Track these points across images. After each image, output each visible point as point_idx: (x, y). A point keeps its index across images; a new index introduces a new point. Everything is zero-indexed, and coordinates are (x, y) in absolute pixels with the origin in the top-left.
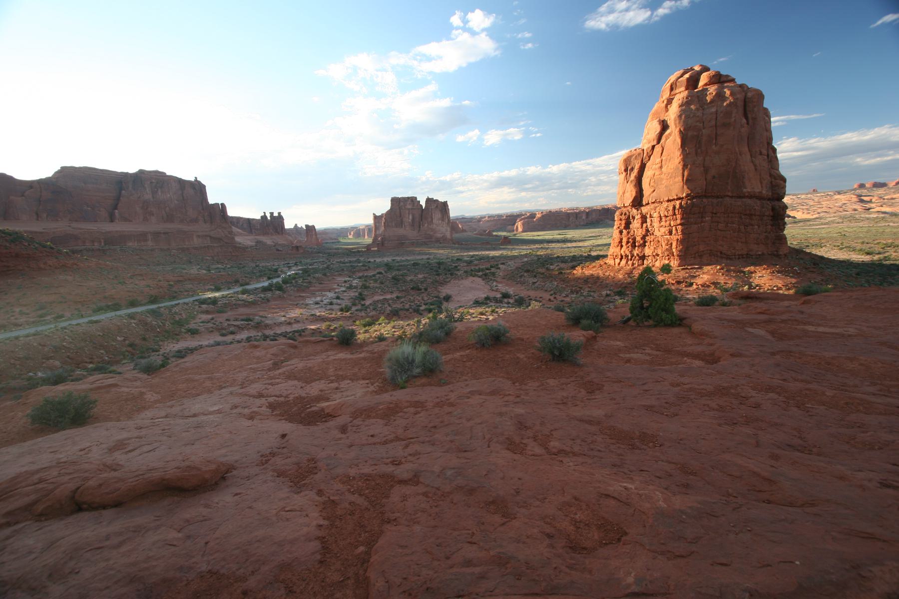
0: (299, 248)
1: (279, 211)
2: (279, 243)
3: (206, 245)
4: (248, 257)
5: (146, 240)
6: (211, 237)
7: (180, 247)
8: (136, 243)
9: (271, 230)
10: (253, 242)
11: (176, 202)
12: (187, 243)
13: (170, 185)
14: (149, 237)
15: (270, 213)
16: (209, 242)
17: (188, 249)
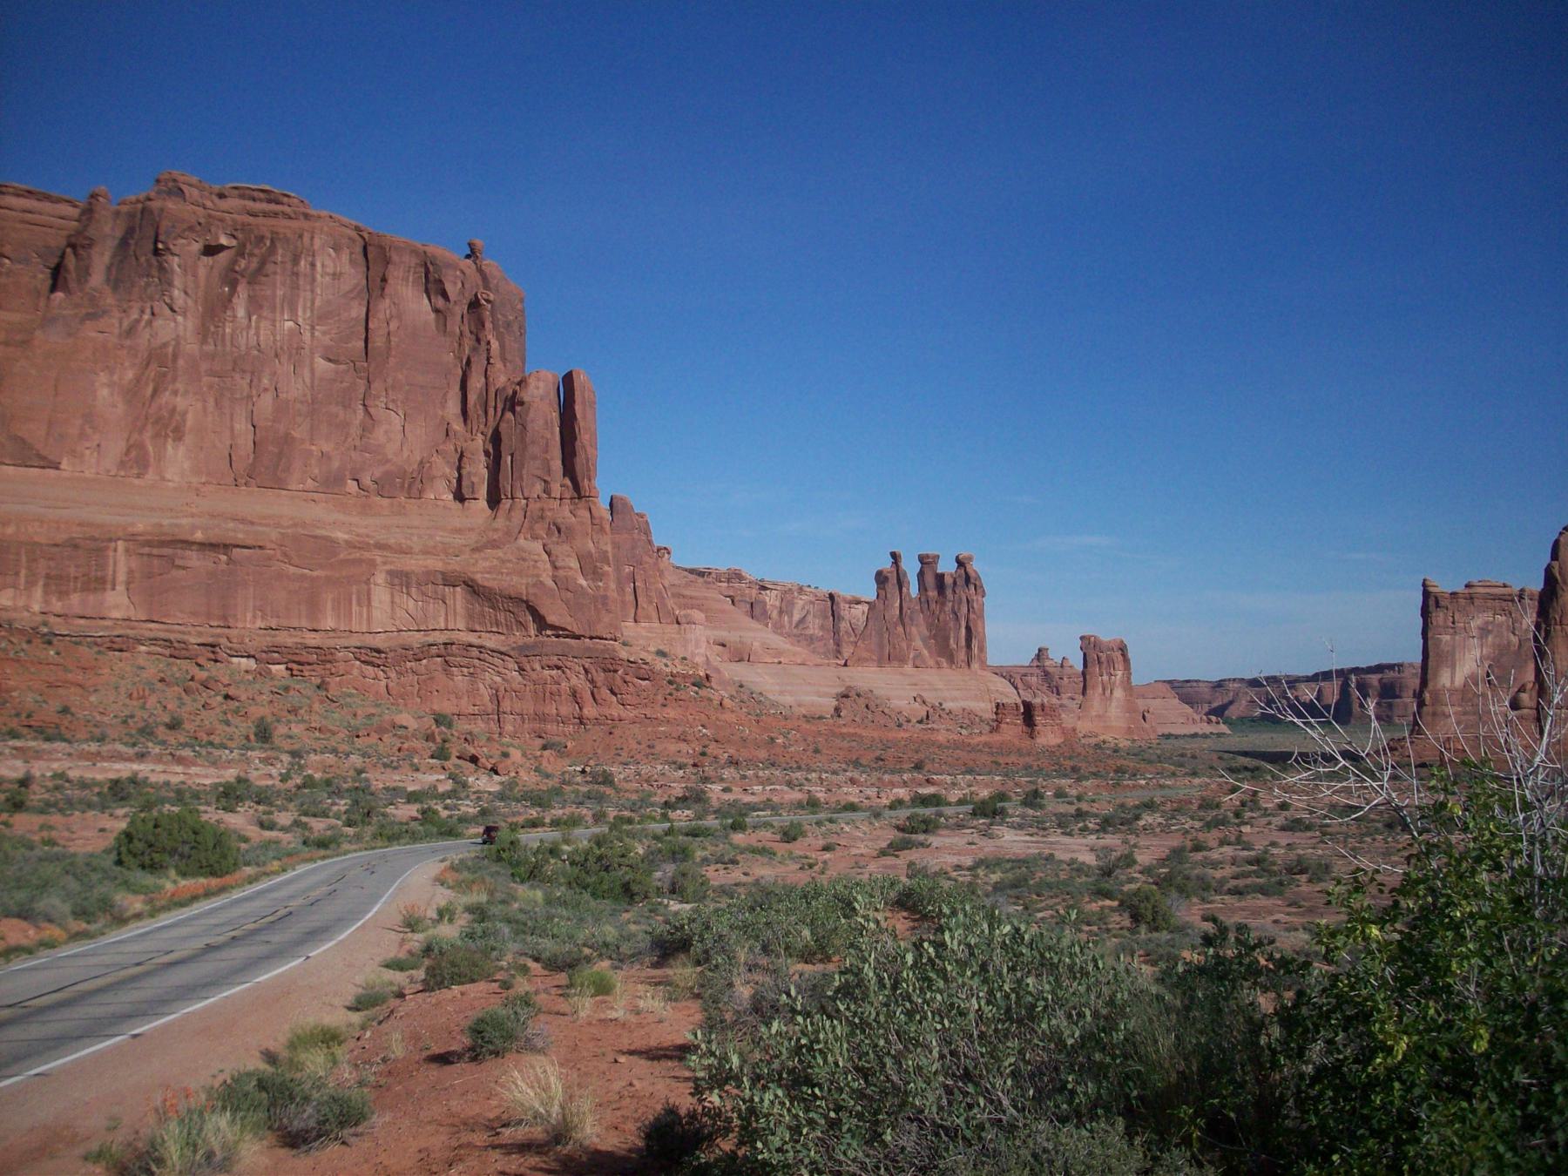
0: (1038, 719)
1: (964, 553)
2: (948, 705)
3: (440, 638)
4: (682, 738)
5: (98, 583)
6: (473, 588)
7: (284, 638)
8: (38, 592)
9: (918, 643)
10: (826, 695)
11: (321, 364)
12: (329, 622)
13: (303, 264)
14: (121, 563)
15: (922, 559)
16: (461, 626)
17: (325, 656)
